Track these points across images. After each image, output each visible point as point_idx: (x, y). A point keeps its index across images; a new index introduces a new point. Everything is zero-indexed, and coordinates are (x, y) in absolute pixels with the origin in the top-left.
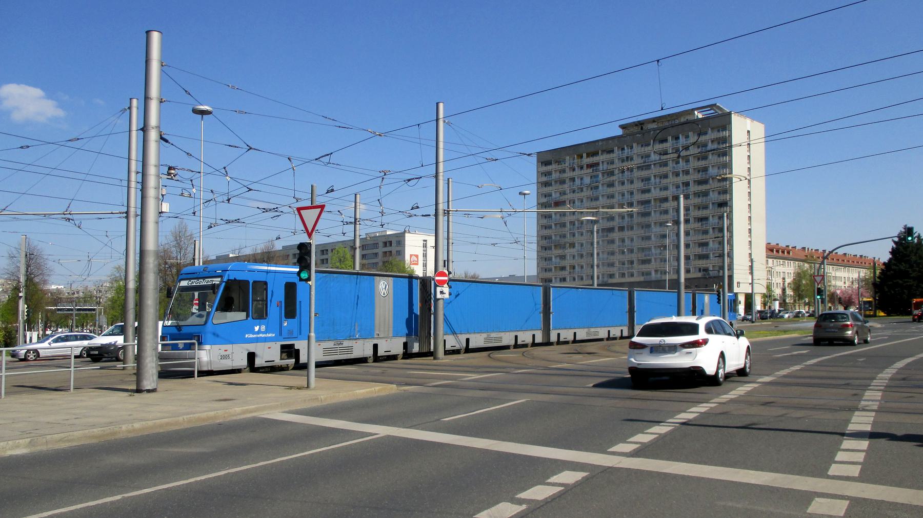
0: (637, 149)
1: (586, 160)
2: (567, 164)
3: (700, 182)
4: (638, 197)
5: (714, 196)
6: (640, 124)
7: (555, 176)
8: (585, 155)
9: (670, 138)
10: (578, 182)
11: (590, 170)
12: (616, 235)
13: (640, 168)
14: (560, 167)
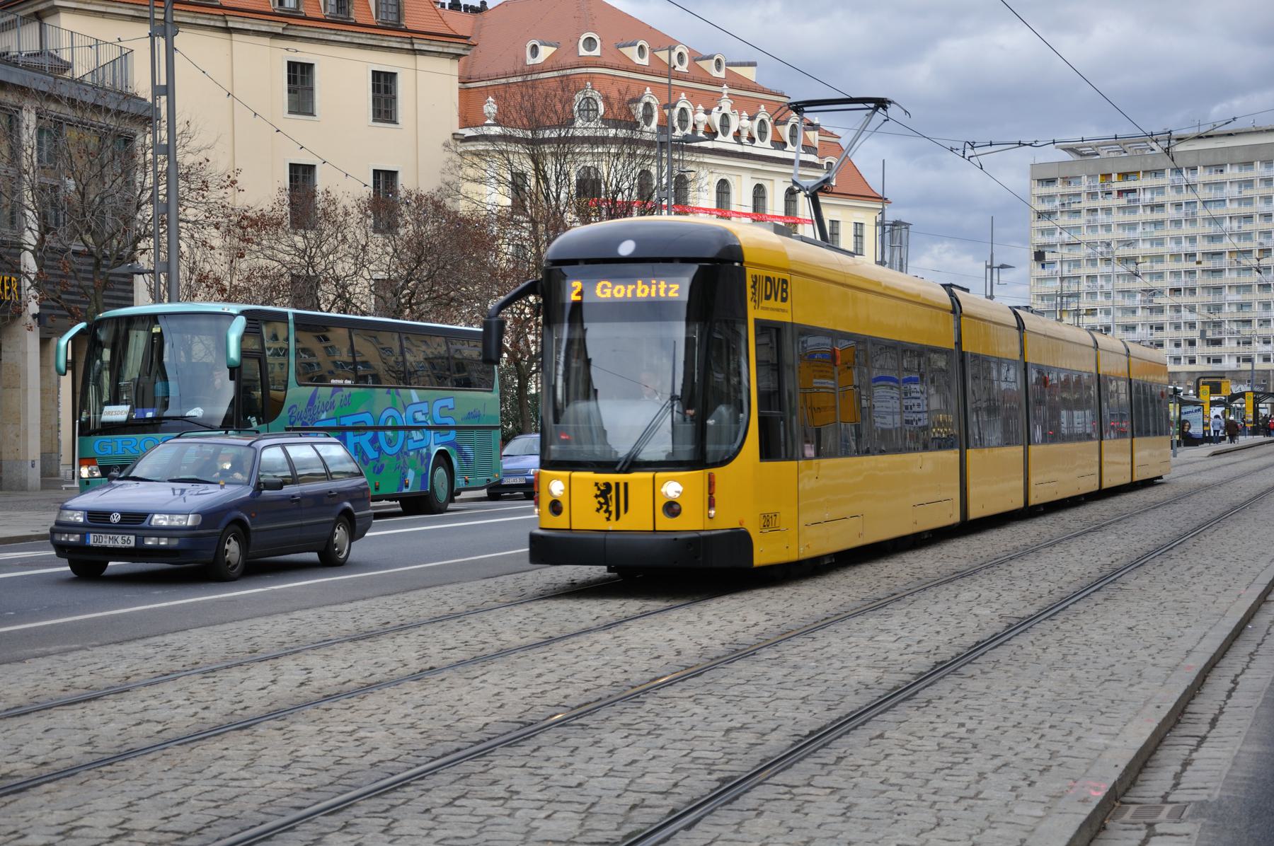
1: (1118, 185)
4: (1202, 246)
8: (1115, 177)
10: (1101, 217)
11: (1123, 201)
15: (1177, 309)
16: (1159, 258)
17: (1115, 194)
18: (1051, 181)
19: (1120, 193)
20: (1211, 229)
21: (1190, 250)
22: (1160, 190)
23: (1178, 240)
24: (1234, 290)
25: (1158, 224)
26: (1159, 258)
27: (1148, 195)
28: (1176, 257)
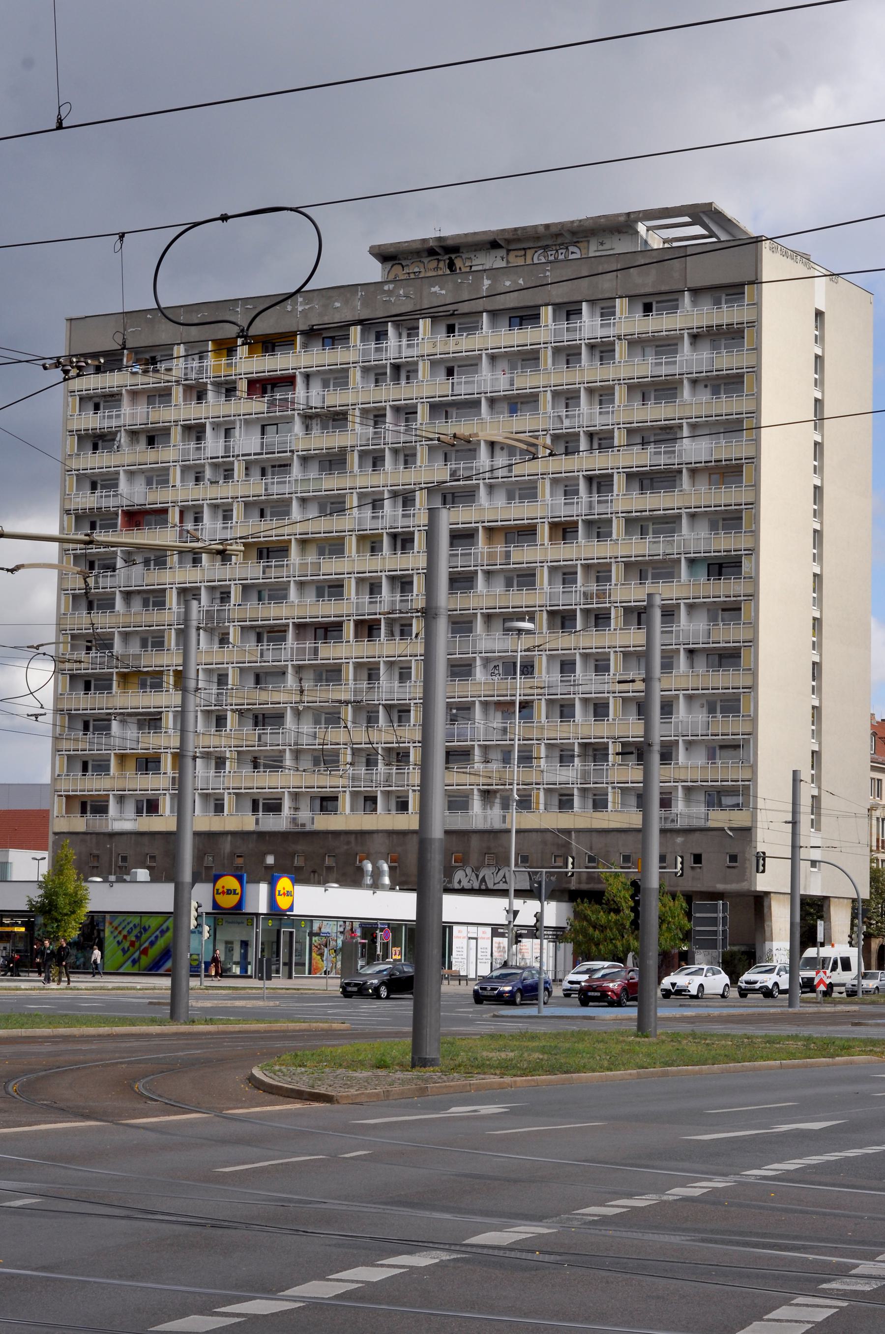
0: (429, 341)
3: (645, 480)
5: (694, 539)
6: (446, 252)
7: (131, 414)
10: (213, 445)
11: (258, 406)
12: (347, 650)
14: (149, 381)
15: (370, 671)
16: (333, 546)
25: (334, 461)
26: (333, 546)
27: (316, 389)
28: (371, 543)
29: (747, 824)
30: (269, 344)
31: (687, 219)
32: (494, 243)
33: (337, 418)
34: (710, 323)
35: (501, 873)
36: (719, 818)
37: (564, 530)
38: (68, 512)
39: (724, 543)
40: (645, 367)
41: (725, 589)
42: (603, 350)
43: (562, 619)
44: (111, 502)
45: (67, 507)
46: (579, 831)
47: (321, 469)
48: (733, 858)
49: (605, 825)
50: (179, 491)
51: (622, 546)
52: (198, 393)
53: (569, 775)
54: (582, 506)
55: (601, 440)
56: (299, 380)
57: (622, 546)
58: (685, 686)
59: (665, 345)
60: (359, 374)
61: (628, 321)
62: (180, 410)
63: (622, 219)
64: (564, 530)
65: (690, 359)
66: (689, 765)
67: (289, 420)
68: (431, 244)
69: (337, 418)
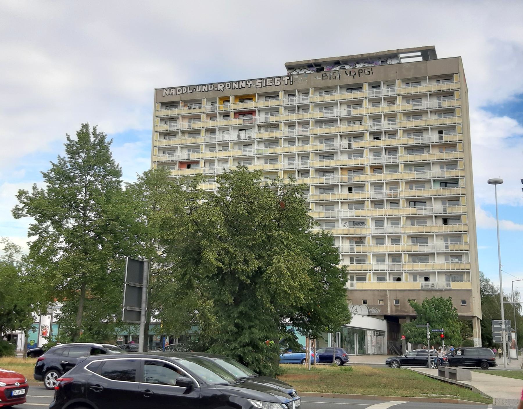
0: (313, 97)
1: (234, 106)
2: (201, 110)
6: (318, 66)
7: (182, 125)
8: (232, 99)
9: (366, 86)
10: (219, 137)
11: (240, 121)
13: (319, 122)
17: (232, 115)
18: (173, 105)
19: (239, 114)
20: (322, 147)
21: (303, 167)
22: (275, 111)
23: (291, 157)
24: (346, 207)
29: (470, 288)
30: (242, 99)
31: (419, 54)
32: (337, 63)
33: (274, 126)
34: (439, 89)
35: (355, 308)
36: (455, 285)
37: (376, 169)
38: (155, 162)
39: (449, 174)
40: (411, 107)
41: (451, 191)
42: (391, 101)
43: (378, 203)
44: (174, 159)
45: (154, 160)
46: (390, 290)
47: (266, 146)
48: (464, 302)
49: (402, 288)
50: (205, 154)
51: (403, 175)
52: (212, 117)
53: (385, 266)
54: (384, 159)
55: (392, 134)
56: (257, 112)
57: (403, 175)
58: (437, 231)
59: (417, 98)
60: (283, 110)
61: (400, 89)
62: (205, 123)
63: (395, 52)
64: (376, 169)
65: (431, 103)
66: (439, 263)
67: (254, 126)
68: (312, 62)
69: (274, 126)
